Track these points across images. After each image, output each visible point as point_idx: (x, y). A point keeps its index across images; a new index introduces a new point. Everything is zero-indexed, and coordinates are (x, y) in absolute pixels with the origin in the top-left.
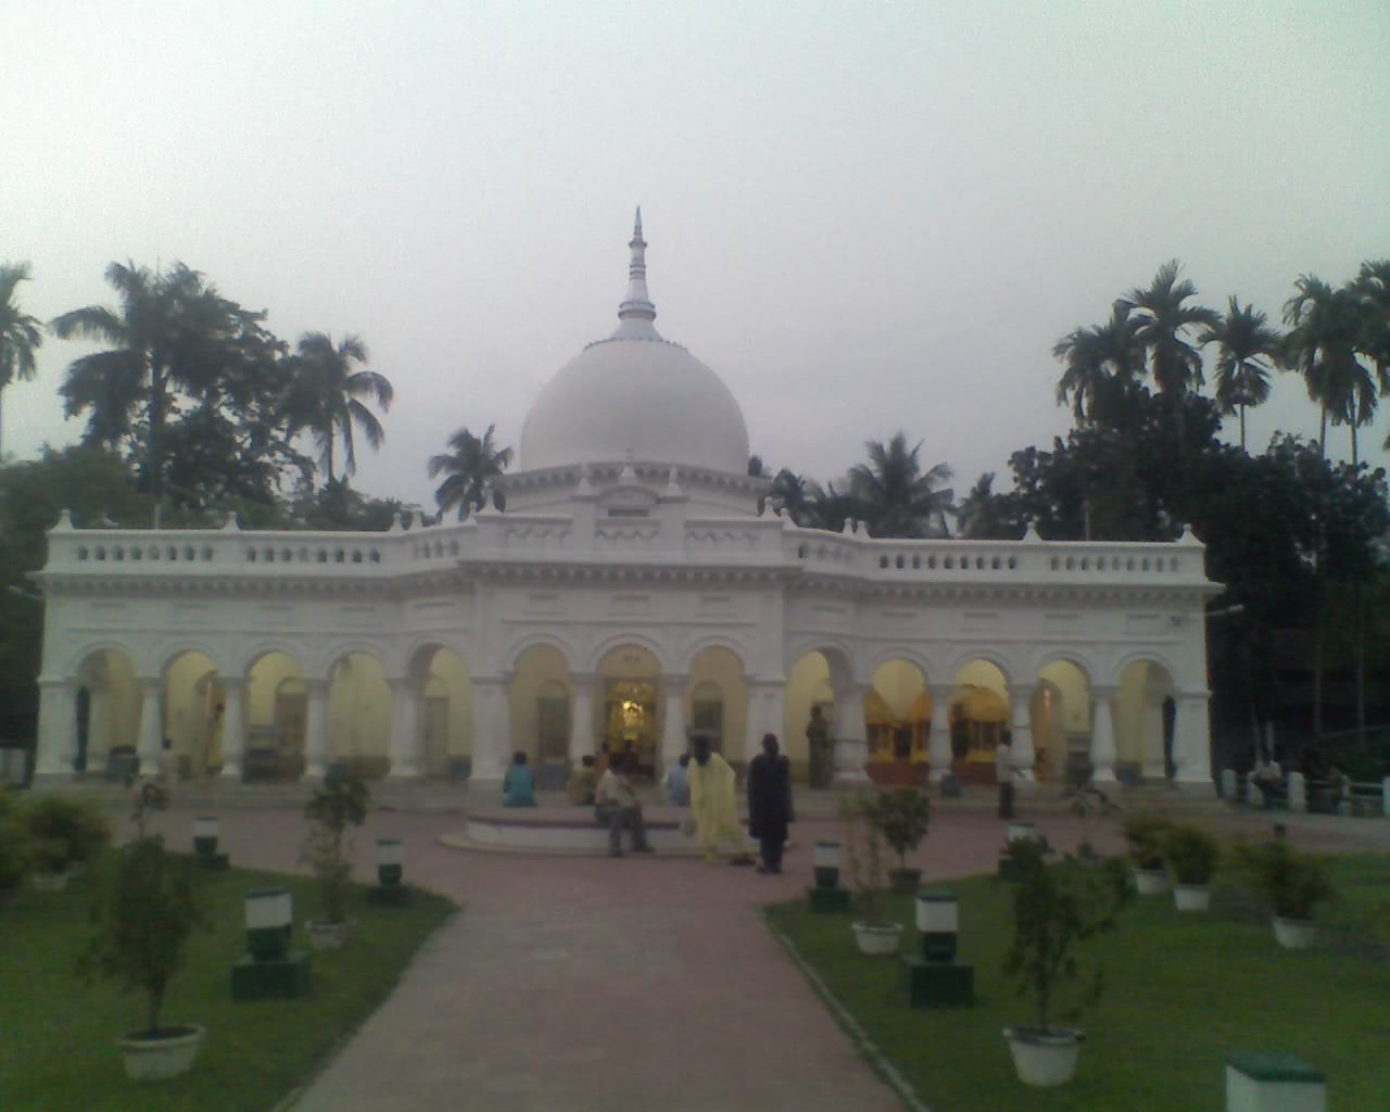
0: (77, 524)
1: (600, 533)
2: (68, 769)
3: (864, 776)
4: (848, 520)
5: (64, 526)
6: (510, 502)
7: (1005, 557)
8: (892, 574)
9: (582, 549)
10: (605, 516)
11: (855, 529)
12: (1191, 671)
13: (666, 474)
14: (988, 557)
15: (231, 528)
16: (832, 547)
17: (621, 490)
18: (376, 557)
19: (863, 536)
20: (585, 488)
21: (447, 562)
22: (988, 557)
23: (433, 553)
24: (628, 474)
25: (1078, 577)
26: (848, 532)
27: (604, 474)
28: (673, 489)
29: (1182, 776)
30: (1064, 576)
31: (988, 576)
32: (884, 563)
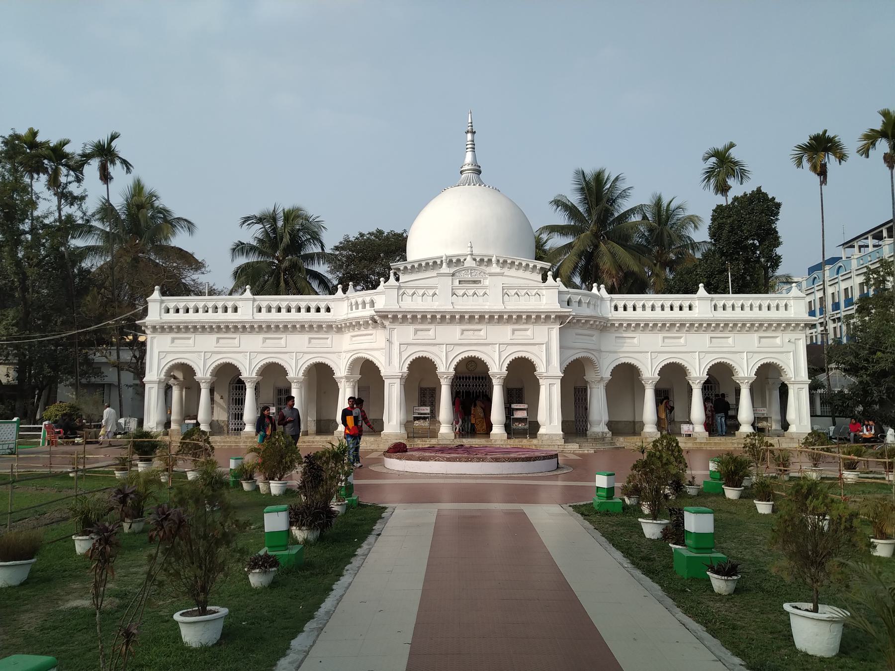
0: (163, 293)
1: (453, 294)
2: (161, 429)
3: (606, 430)
4: (595, 285)
5: (156, 295)
6: (403, 278)
7: (686, 304)
8: (621, 314)
9: (442, 303)
10: (456, 283)
11: (599, 290)
12: (796, 369)
13: (490, 261)
14: (676, 305)
15: (248, 294)
16: (585, 300)
17: (467, 269)
18: (328, 310)
19: (603, 292)
20: (445, 269)
21: (369, 312)
22: (676, 305)
23: (360, 306)
24: (469, 262)
25: (729, 314)
26: (595, 290)
27: (455, 262)
28: (495, 268)
29: (793, 429)
30: (720, 315)
31: (676, 314)
32: (616, 308)
